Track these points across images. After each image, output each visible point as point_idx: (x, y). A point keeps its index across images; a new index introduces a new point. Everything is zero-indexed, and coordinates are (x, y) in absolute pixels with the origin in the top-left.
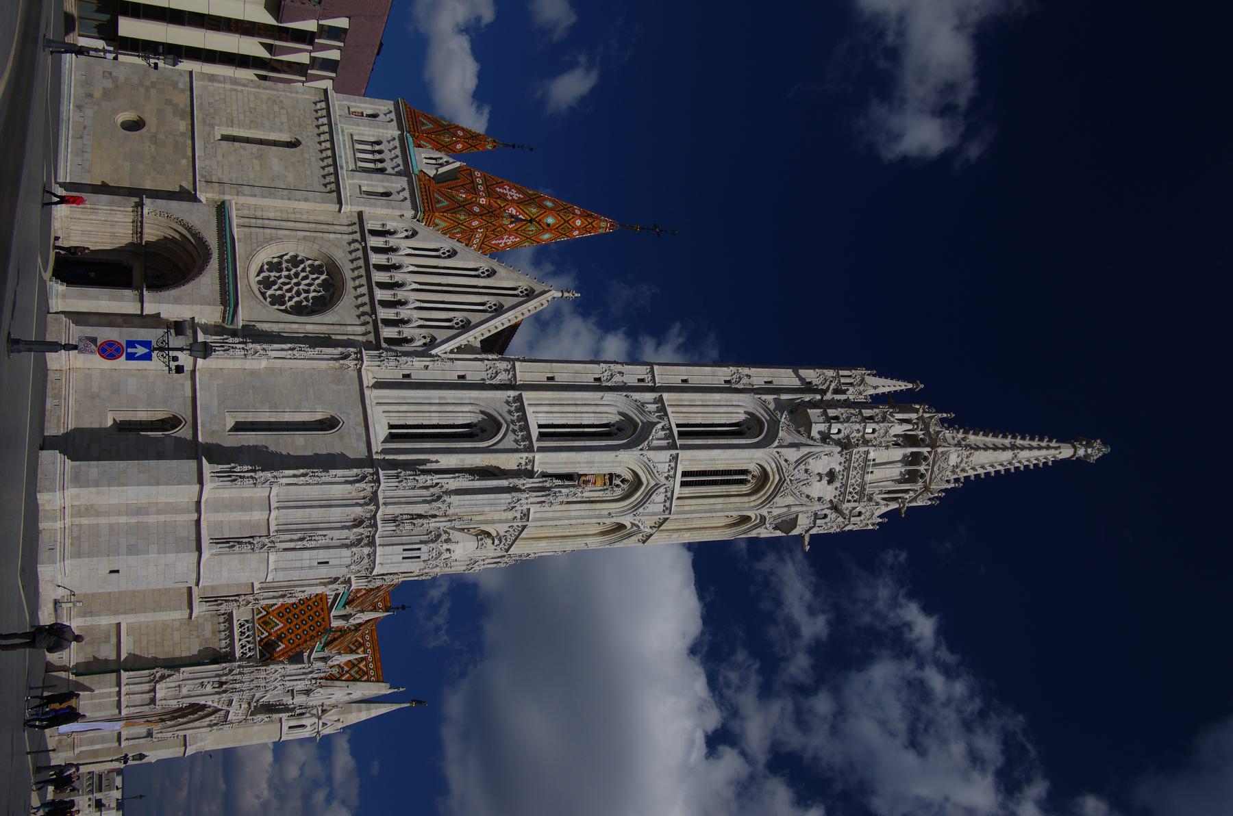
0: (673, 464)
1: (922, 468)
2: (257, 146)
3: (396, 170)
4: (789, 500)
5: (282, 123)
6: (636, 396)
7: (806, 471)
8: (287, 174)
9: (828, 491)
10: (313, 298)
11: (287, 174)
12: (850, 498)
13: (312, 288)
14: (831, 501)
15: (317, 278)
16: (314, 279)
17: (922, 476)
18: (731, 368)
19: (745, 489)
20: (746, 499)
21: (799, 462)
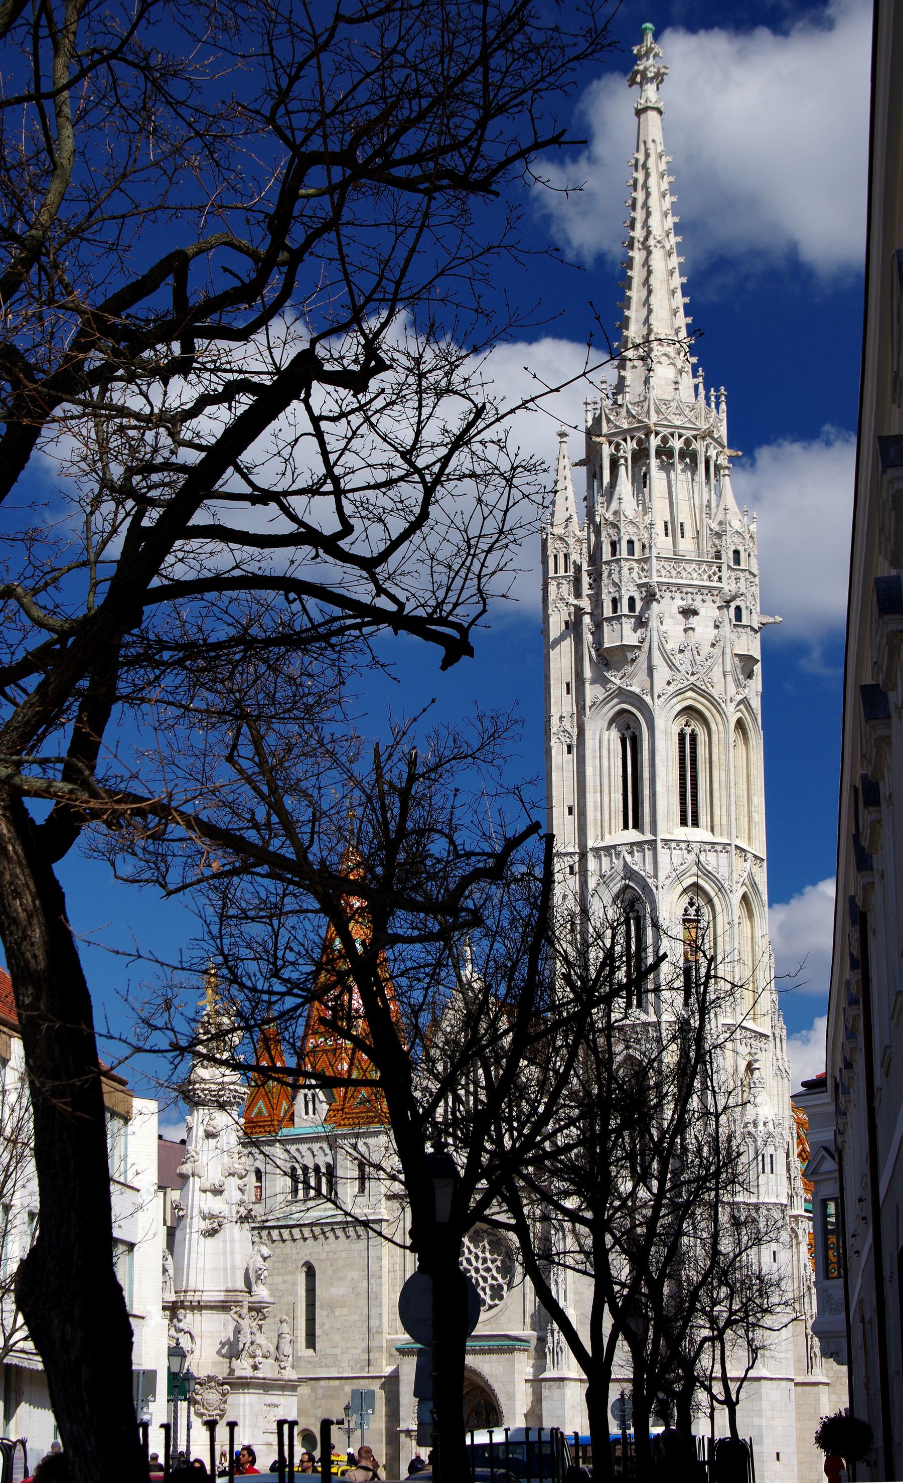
0: (673, 845)
1: (677, 444)
2: (317, 1311)
3: (328, 1151)
4: (716, 674)
5: (285, 1282)
6: (592, 883)
7: (681, 651)
8: (349, 1278)
9: (708, 611)
10: (491, 1253)
11: (349, 1278)
12: (716, 578)
13: (480, 1254)
14: (719, 608)
15: (468, 1248)
16: (470, 1252)
17: (688, 442)
18: (552, 743)
19: (702, 738)
20: (715, 737)
21: (671, 666)
